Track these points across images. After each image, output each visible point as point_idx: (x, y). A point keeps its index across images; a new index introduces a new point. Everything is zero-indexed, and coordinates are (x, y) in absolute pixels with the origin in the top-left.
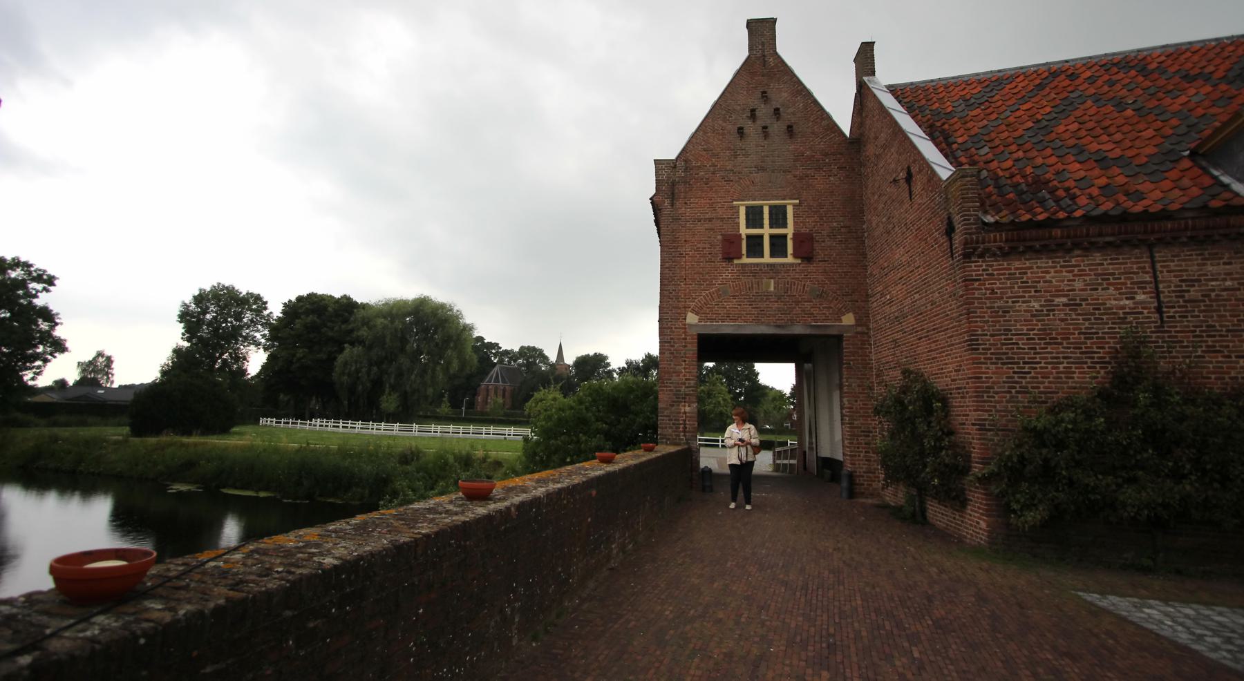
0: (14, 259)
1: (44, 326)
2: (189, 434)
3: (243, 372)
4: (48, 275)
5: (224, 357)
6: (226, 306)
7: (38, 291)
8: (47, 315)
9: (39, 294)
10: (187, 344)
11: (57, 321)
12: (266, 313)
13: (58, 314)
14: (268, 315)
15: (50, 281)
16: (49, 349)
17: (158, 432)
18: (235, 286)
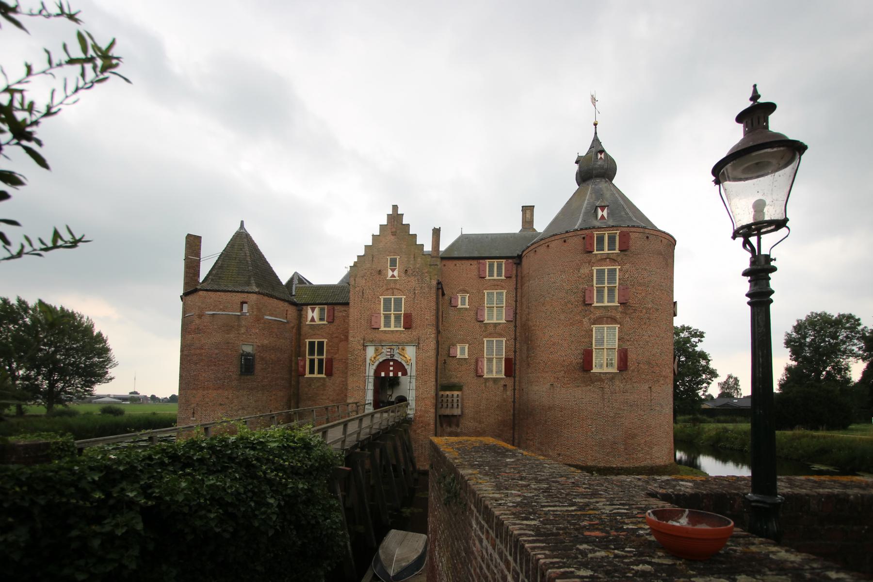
0: (681, 326)
1: (703, 363)
2: (817, 429)
3: (848, 380)
4: (700, 332)
5: (828, 369)
6: (822, 329)
7: (696, 343)
8: (703, 356)
9: (697, 344)
10: (794, 363)
11: (709, 358)
12: (860, 328)
13: (709, 354)
14: (863, 330)
15: (701, 335)
16: (708, 376)
17: (792, 428)
18: (826, 311)
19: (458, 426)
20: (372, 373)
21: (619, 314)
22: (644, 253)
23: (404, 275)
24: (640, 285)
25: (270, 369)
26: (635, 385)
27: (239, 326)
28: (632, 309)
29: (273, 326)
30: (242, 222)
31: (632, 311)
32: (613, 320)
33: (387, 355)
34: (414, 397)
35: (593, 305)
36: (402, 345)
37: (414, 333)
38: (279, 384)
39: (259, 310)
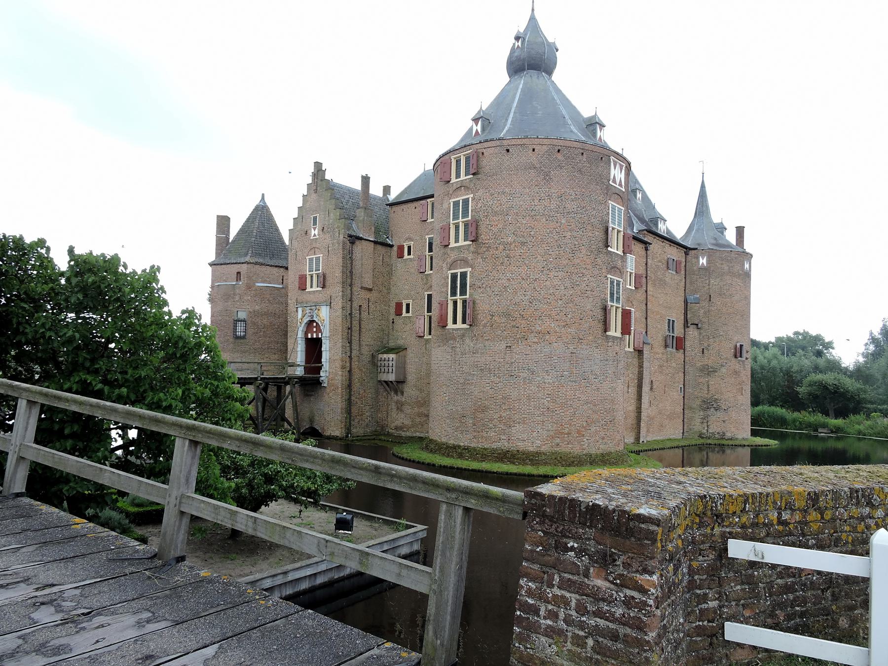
19: (402, 393)
20: (300, 334)
21: (471, 255)
22: (501, 172)
23: (321, 232)
24: (496, 213)
25: (262, 333)
26: (487, 343)
27: (234, 294)
28: (485, 247)
29: (264, 293)
30: (263, 195)
31: (485, 249)
32: (465, 262)
33: (309, 316)
34: (328, 358)
35: (449, 246)
36: (317, 305)
37: (328, 291)
38: (273, 347)
39: (249, 278)
